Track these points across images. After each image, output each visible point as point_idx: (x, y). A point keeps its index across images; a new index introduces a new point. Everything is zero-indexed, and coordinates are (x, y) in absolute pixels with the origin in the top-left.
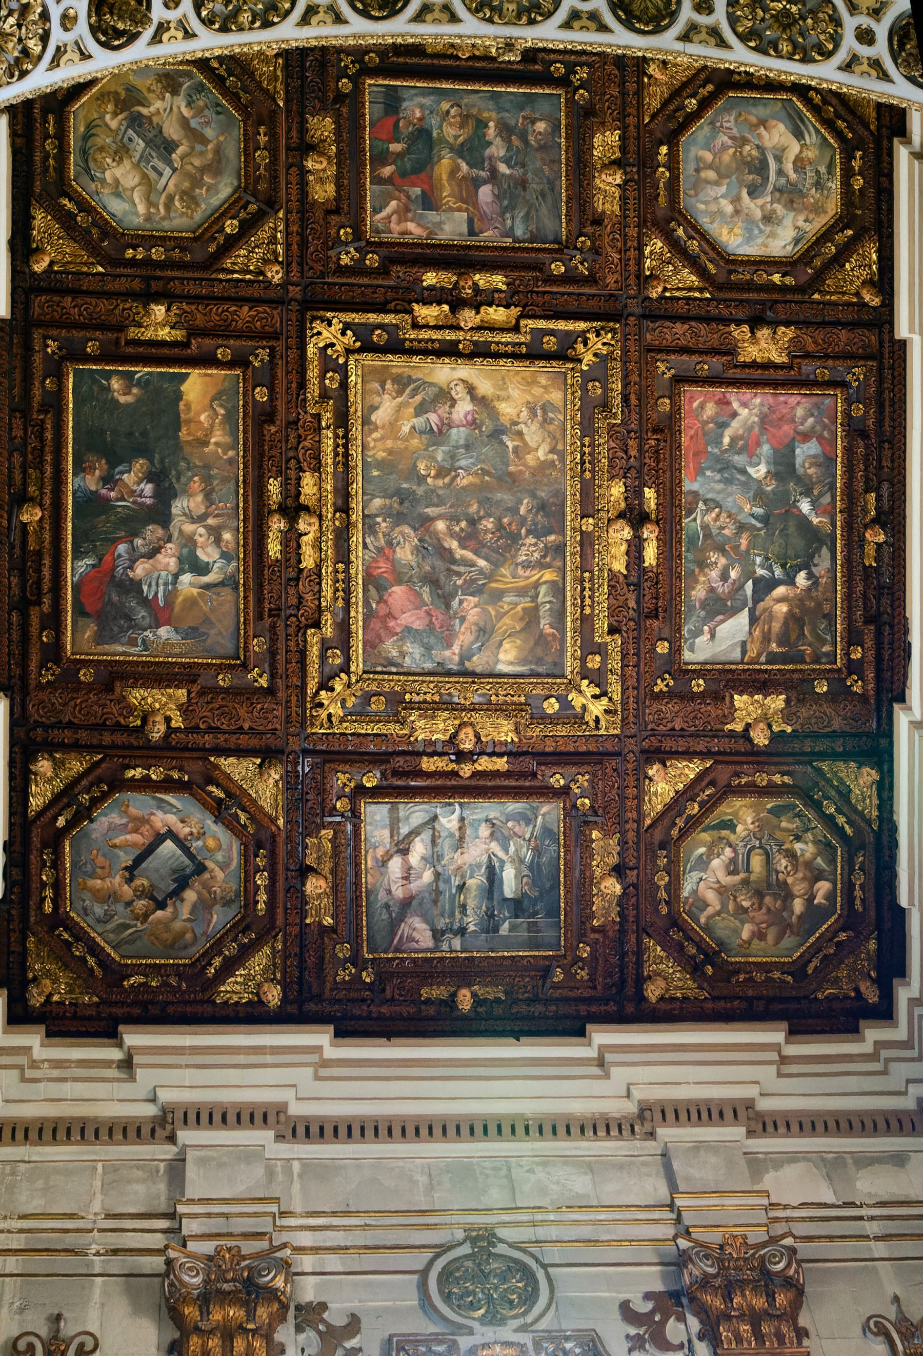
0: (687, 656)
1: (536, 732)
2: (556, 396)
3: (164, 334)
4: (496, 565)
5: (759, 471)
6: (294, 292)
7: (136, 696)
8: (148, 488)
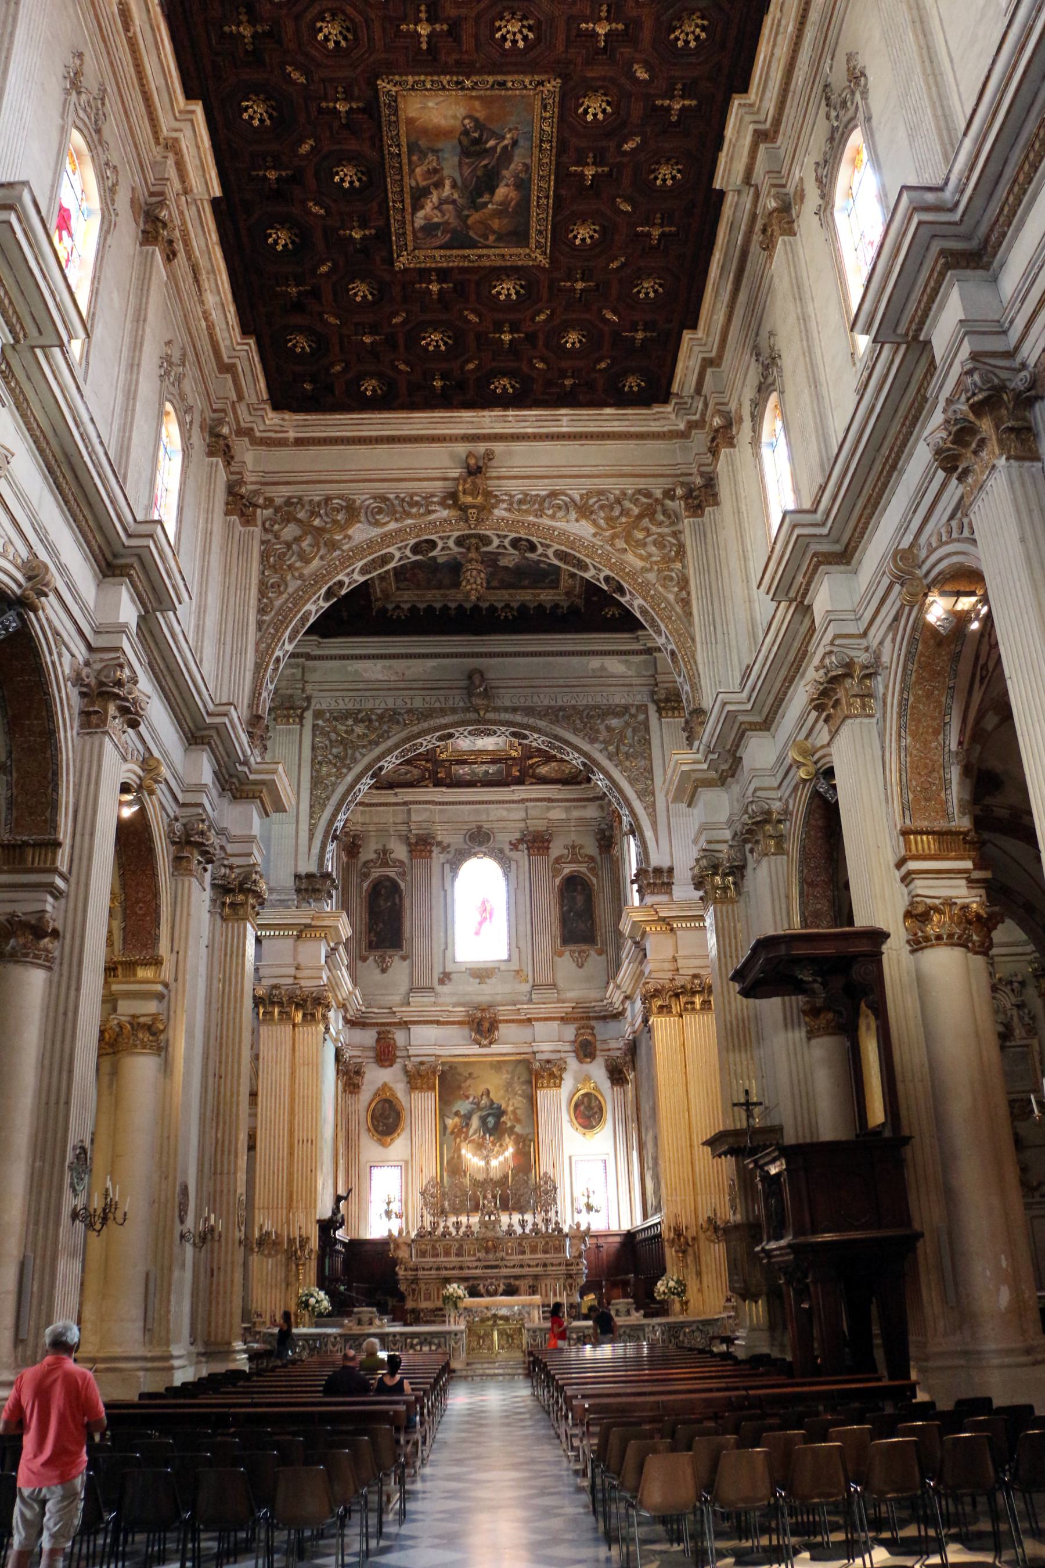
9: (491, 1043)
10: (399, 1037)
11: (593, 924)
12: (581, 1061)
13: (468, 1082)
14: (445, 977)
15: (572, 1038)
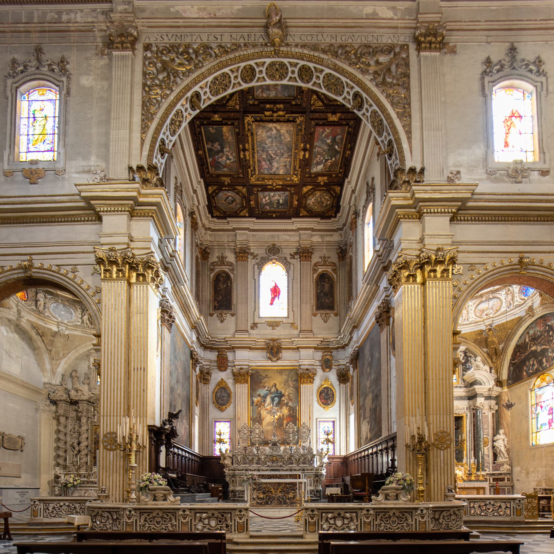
0: (312, 171)
1: (285, 183)
2: (292, 129)
3: (218, 119)
4: (280, 158)
5: (329, 141)
6: (242, 109)
7: (222, 178)
8: (219, 147)
9: (278, 360)
10: (230, 356)
11: (333, 300)
12: (324, 371)
13: (265, 380)
14: (255, 326)
15: (320, 359)
